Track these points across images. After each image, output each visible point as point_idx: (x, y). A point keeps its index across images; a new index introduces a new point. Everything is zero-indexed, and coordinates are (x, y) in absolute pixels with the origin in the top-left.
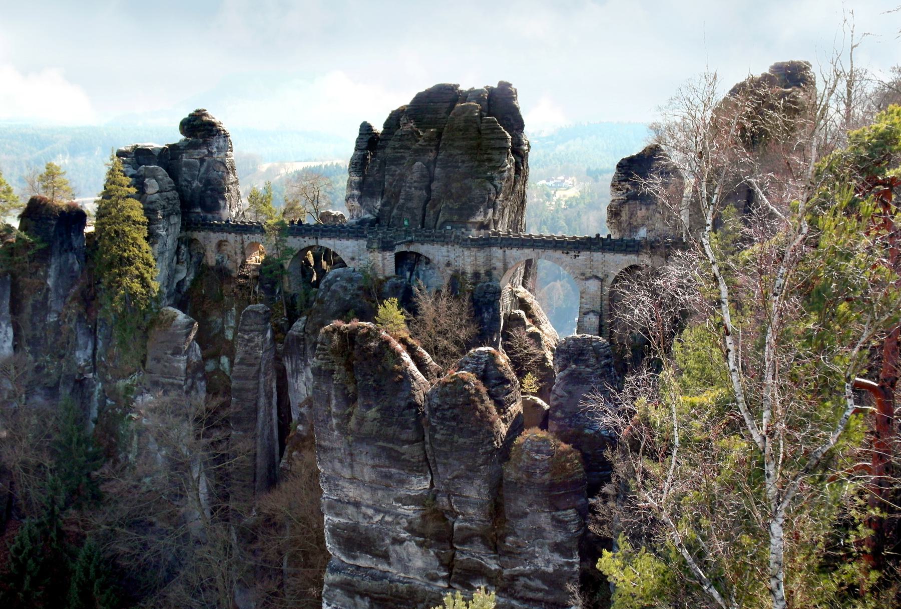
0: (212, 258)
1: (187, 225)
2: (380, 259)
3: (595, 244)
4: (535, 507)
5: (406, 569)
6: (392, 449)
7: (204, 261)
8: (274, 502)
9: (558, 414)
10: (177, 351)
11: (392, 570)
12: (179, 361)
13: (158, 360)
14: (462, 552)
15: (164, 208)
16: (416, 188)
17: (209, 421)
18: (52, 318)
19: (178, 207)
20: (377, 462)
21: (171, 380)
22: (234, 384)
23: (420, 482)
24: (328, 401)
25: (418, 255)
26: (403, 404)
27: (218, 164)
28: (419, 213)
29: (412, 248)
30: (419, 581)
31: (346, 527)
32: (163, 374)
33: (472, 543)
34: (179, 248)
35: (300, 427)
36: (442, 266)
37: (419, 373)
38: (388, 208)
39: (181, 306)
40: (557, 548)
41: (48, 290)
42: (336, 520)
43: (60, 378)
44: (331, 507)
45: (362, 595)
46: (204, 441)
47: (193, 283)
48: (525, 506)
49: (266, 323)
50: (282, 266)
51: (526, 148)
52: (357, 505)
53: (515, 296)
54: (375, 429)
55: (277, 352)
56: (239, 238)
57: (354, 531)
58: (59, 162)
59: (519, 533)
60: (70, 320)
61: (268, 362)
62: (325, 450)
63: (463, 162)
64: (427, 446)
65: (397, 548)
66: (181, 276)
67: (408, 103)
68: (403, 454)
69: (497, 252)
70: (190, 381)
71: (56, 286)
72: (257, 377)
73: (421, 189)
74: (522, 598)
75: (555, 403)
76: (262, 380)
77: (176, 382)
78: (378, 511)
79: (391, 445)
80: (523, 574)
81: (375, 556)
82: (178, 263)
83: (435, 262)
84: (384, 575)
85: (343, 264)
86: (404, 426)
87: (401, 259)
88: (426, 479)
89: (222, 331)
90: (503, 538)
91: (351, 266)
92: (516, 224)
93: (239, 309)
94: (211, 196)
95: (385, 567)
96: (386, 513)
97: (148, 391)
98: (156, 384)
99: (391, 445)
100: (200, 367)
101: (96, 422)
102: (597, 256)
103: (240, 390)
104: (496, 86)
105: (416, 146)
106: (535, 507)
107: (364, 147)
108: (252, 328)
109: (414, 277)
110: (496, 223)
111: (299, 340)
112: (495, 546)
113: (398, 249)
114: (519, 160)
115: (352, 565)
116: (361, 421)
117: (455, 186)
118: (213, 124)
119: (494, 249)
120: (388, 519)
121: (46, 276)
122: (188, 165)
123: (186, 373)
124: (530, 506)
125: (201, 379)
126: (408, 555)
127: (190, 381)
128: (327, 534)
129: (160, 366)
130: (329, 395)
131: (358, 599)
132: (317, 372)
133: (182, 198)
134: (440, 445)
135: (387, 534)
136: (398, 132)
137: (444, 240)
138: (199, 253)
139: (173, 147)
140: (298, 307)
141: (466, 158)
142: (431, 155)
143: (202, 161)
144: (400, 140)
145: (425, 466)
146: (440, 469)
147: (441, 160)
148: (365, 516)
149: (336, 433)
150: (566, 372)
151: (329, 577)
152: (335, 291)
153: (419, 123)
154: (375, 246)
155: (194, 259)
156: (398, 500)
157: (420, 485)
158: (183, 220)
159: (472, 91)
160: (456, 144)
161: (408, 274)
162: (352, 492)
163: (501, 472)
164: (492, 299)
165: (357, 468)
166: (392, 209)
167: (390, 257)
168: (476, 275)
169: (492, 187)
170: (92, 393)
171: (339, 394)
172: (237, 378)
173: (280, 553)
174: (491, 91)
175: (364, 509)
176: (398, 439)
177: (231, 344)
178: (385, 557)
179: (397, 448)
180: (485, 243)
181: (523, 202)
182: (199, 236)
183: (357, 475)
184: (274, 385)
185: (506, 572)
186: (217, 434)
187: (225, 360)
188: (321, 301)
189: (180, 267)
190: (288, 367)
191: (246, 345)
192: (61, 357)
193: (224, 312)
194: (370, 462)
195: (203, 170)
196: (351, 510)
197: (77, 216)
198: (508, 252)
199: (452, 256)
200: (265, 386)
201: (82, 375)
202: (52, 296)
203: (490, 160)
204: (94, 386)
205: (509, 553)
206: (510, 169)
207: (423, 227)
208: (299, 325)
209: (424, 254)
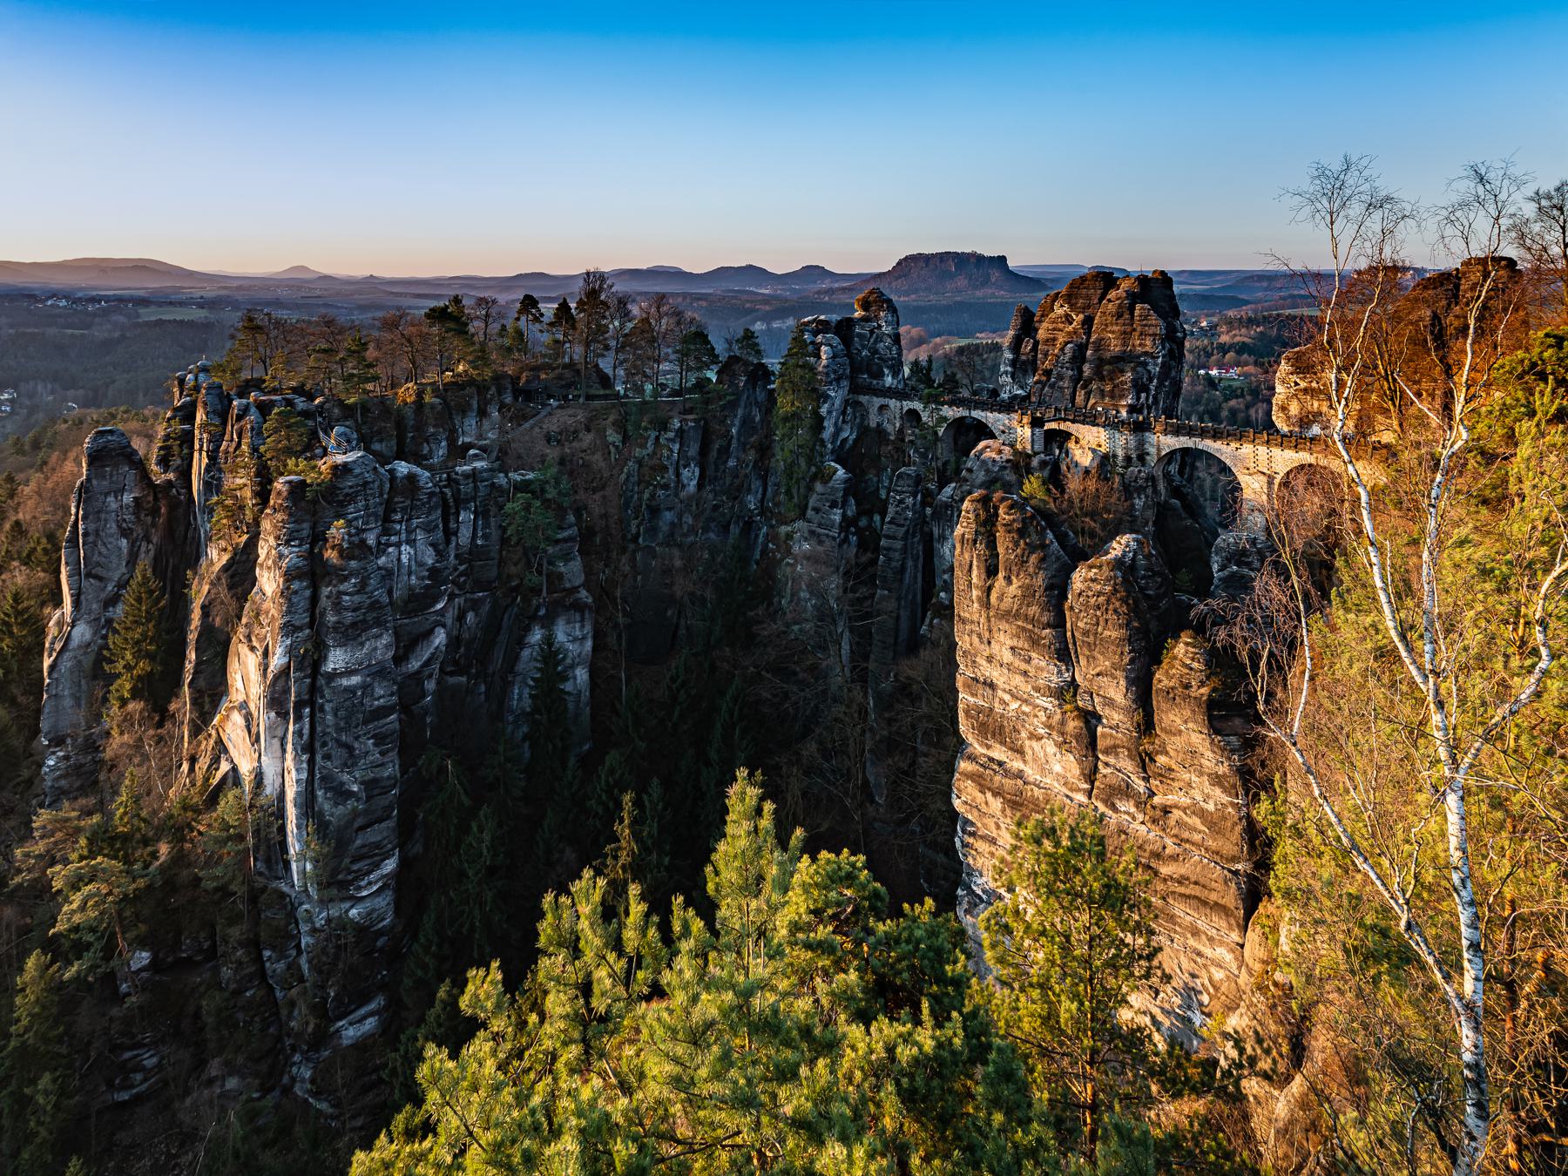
1: (855, 389)
4: (1190, 725)
8: (912, 669)
10: (834, 505)
11: (1031, 772)
13: (817, 510)
14: (1107, 764)
17: (857, 577)
18: (731, 463)
22: (883, 542)
30: (1058, 787)
31: (980, 710)
32: (820, 525)
35: (942, 594)
44: (967, 686)
45: (996, 794)
46: (850, 595)
47: (855, 441)
48: (1179, 721)
52: (992, 686)
65: (1034, 744)
66: (845, 435)
81: (1011, 749)
84: (1019, 775)
89: (878, 489)
93: (894, 471)
95: (1021, 765)
96: (1025, 701)
97: (806, 539)
98: (812, 533)
101: (757, 563)
103: (889, 549)
106: (1190, 725)
111: (947, 506)
120: (1026, 708)
121: (733, 425)
122: (860, 335)
131: (989, 795)
133: (852, 364)
143: (872, 332)
156: (1037, 689)
170: (757, 536)
171: (982, 566)
173: (914, 727)
175: (1000, 693)
177: (885, 503)
178: (1020, 751)
182: (863, 399)
186: (863, 591)
187: (877, 518)
188: (970, 470)
190: (936, 531)
192: (735, 498)
193: (880, 470)
202: (734, 441)
208: (948, 490)
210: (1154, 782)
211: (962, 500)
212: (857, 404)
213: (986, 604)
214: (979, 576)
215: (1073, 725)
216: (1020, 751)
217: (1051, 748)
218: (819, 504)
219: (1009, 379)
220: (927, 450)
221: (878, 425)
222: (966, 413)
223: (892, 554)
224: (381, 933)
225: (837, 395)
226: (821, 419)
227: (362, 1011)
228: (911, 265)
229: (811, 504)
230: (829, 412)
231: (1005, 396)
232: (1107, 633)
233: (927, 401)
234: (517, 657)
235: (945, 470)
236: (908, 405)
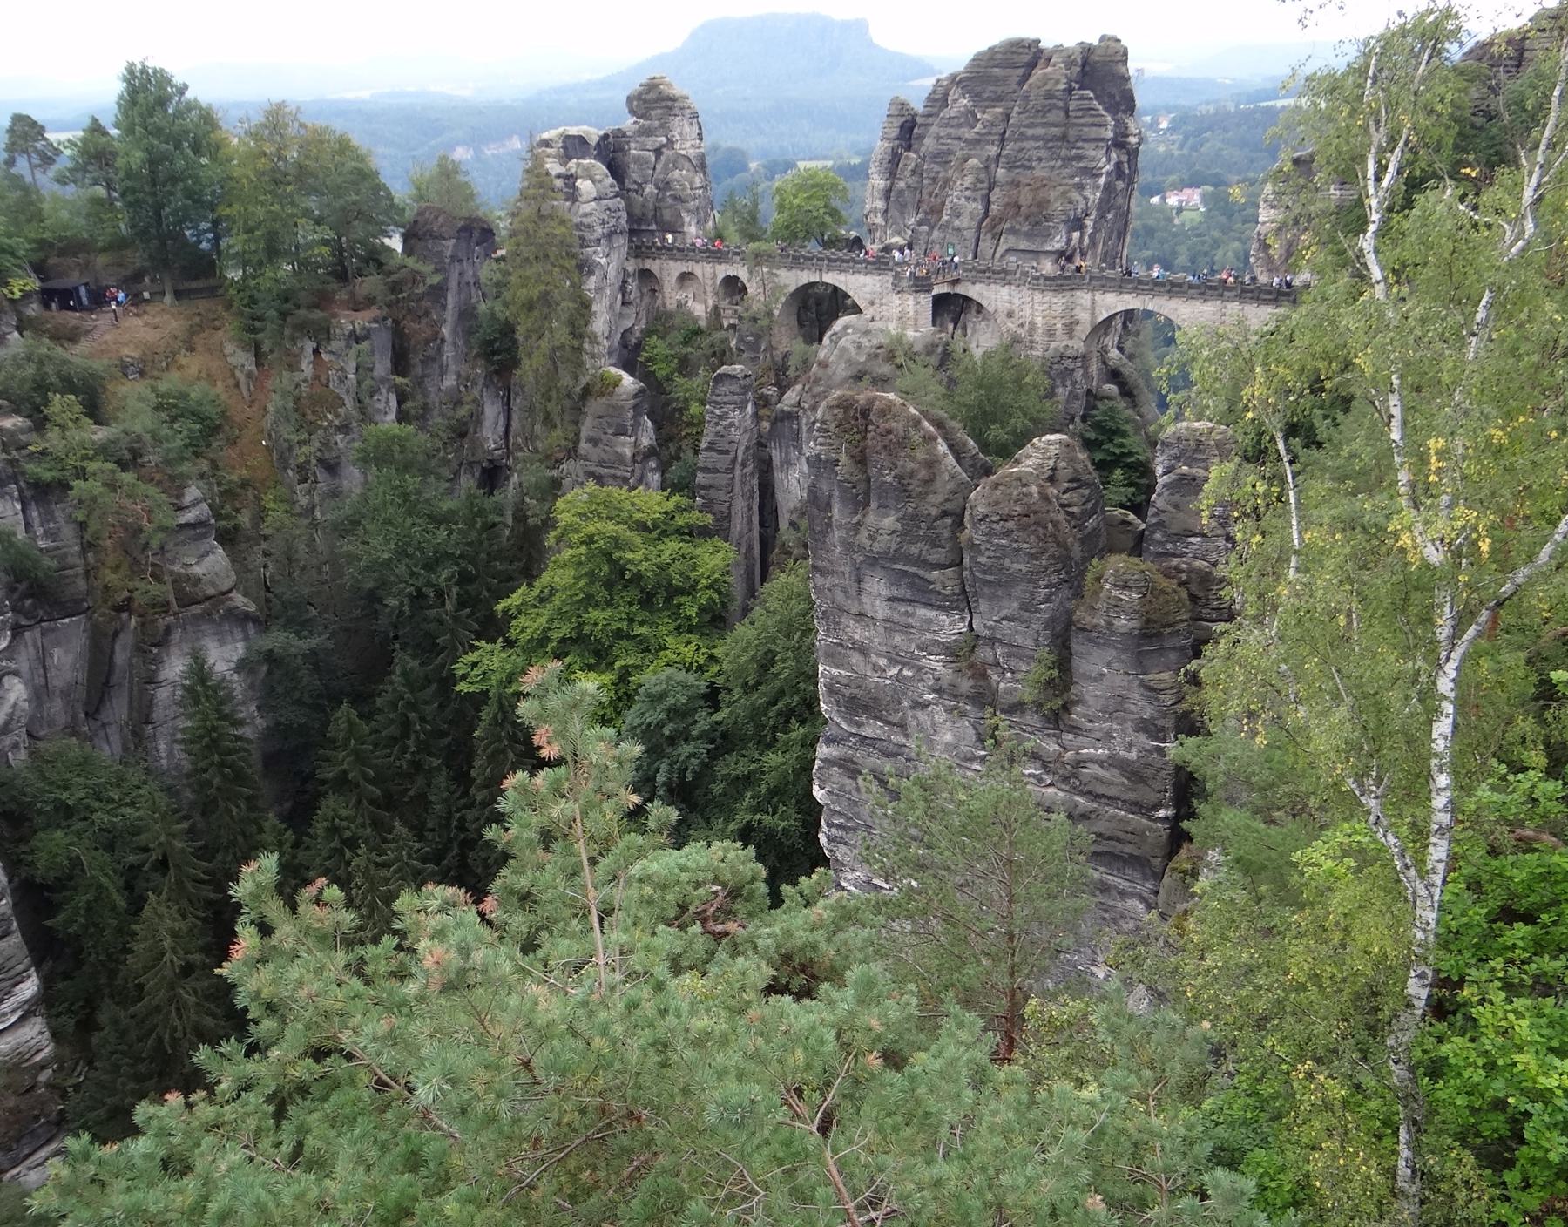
0: (672, 296)
1: (637, 251)
2: (911, 302)
3: (1230, 289)
5: (930, 743)
6: (915, 575)
7: (659, 302)
9: (1158, 536)
10: (621, 431)
12: (623, 444)
13: (594, 441)
15: (604, 223)
16: (967, 198)
18: (450, 381)
19: (623, 222)
20: (895, 592)
21: (612, 471)
22: (700, 478)
23: (953, 623)
24: (829, 506)
25: (967, 299)
26: (934, 512)
27: (681, 160)
28: (970, 235)
29: (960, 289)
33: (1023, 712)
34: (625, 282)
36: (1001, 318)
37: (958, 468)
38: (926, 228)
39: (629, 366)
40: (1144, 726)
41: (443, 340)
42: (835, 672)
43: (460, 465)
49: (744, 394)
50: (770, 314)
51: (1133, 140)
52: (864, 651)
53: (1104, 363)
54: (894, 546)
55: (760, 435)
56: (708, 268)
57: (859, 687)
58: (461, 154)
59: (1091, 701)
60: (475, 384)
61: (747, 448)
62: (824, 573)
63: (1040, 159)
64: (966, 573)
65: (919, 714)
66: (628, 324)
67: (962, 69)
68: (930, 583)
69: (1084, 297)
70: (638, 472)
71: (454, 331)
72: (730, 470)
73: (975, 200)
74: (1090, 793)
75: (1154, 520)
76: (738, 473)
77: (619, 473)
78: (893, 662)
79: (914, 570)
80: (1093, 760)
81: (888, 723)
82: (623, 304)
83: (991, 310)
85: (856, 310)
86: (934, 543)
87: (940, 303)
88: (963, 619)
90: (1066, 708)
91: (869, 313)
92: (1111, 258)
94: (670, 207)
95: (902, 739)
96: (904, 664)
99: (914, 570)
100: (651, 453)
102: (1234, 307)
103: (707, 488)
104: (1095, 42)
105: (969, 134)
107: (893, 135)
108: (726, 399)
109: (959, 332)
110: (1083, 254)
111: (790, 417)
112: (1057, 720)
113: (938, 290)
114: (1124, 158)
115: (854, 735)
116: (872, 538)
117: (1026, 197)
118: (673, 99)
119: (1078, 293)
120: (905, 672)
122: (637, 159)
123: (635, 461)
124: (1109, 664)
125: (652, 470)
126: (933, 725)
127: (638, 472)
128: (822, 689)
129: (598, 450)
130: (830, 496)
132: (815, 462)
134: (984, 572)
135: (905, 694)
136: (946, 113)
137: (1003, 276)
138: (654, 291)
139: (620, 134)
140: (791, 373)
141: (1043, 153)
142: (993, 150)
143: (658, 152)
144: (947, 125)
145: (962, 602)
146: (983, 605)
147: (1007, 156)
148: (875, 668)
149: (838, 550)
150: (1172, 476)
151: (823, 751)
152: (844, 350)
153: (976, 96)
154: (904, 283)
155: (647, 299)
157: (950, 626)
158: (631, 241)
159: (1058, 49)
160: (1030, 132)
161: (951, 327)
162: (858, 633)
163: (1070, 613)
164: (1071, 367)
165: (865, 599)
166: (932, 228)
167: (926, 301)
168: (1050, 333)
169: (1080, 198)
172: (705, 470)
174: (1087, 50)
175: (874, 657)
176: (925, 562)
178: (902, 726)
179: (922, 573)
180: (1063, 283)
181: (1126, 224)
182: (653, 265)
183: (867, 609)
184: (755, 481)
185: (1069, 755)
188: (824, 365)
189: (626, 310)
191: (717, 424)
192: (463, 435)
194: (885, 593)
195: (659, 167)
196: (855, 658)
197: (479, 233)
198: (1098, 296)
199: (1017, 302)
200: (743, 483)
201: (491, 461)
203: (1080, 158)
204: (507, 478)
205: (1075, 729)
206: (1109, 174)
207: (975, 257)
209: (975, 297)
210: (1068, 737)
211: (814, 408)
212: (645, 275)
213: (850, 547)
214: (840, 511)
215: (966, 685)
216: (902, 726)
217: (940, 714)
218: (596, 433)
219: (879, 220)
220: (758, 337)
221: (680, 305)
222: (814, 278)
223: (713, 494)
224: (43, 1066)
225: (610, 261)
226: (586, 305)
227: (43, 1153)
228: (710, 38)
229: (583, 435)
230: (599, 290)
231: (873, 247)
232: (1016, 566)
233: (758, 258)
234: (150, 704)
235: (785, 368)
236: (723, 270)
